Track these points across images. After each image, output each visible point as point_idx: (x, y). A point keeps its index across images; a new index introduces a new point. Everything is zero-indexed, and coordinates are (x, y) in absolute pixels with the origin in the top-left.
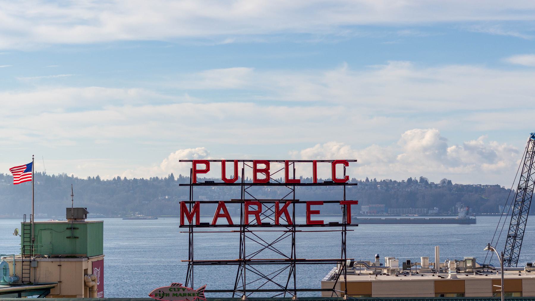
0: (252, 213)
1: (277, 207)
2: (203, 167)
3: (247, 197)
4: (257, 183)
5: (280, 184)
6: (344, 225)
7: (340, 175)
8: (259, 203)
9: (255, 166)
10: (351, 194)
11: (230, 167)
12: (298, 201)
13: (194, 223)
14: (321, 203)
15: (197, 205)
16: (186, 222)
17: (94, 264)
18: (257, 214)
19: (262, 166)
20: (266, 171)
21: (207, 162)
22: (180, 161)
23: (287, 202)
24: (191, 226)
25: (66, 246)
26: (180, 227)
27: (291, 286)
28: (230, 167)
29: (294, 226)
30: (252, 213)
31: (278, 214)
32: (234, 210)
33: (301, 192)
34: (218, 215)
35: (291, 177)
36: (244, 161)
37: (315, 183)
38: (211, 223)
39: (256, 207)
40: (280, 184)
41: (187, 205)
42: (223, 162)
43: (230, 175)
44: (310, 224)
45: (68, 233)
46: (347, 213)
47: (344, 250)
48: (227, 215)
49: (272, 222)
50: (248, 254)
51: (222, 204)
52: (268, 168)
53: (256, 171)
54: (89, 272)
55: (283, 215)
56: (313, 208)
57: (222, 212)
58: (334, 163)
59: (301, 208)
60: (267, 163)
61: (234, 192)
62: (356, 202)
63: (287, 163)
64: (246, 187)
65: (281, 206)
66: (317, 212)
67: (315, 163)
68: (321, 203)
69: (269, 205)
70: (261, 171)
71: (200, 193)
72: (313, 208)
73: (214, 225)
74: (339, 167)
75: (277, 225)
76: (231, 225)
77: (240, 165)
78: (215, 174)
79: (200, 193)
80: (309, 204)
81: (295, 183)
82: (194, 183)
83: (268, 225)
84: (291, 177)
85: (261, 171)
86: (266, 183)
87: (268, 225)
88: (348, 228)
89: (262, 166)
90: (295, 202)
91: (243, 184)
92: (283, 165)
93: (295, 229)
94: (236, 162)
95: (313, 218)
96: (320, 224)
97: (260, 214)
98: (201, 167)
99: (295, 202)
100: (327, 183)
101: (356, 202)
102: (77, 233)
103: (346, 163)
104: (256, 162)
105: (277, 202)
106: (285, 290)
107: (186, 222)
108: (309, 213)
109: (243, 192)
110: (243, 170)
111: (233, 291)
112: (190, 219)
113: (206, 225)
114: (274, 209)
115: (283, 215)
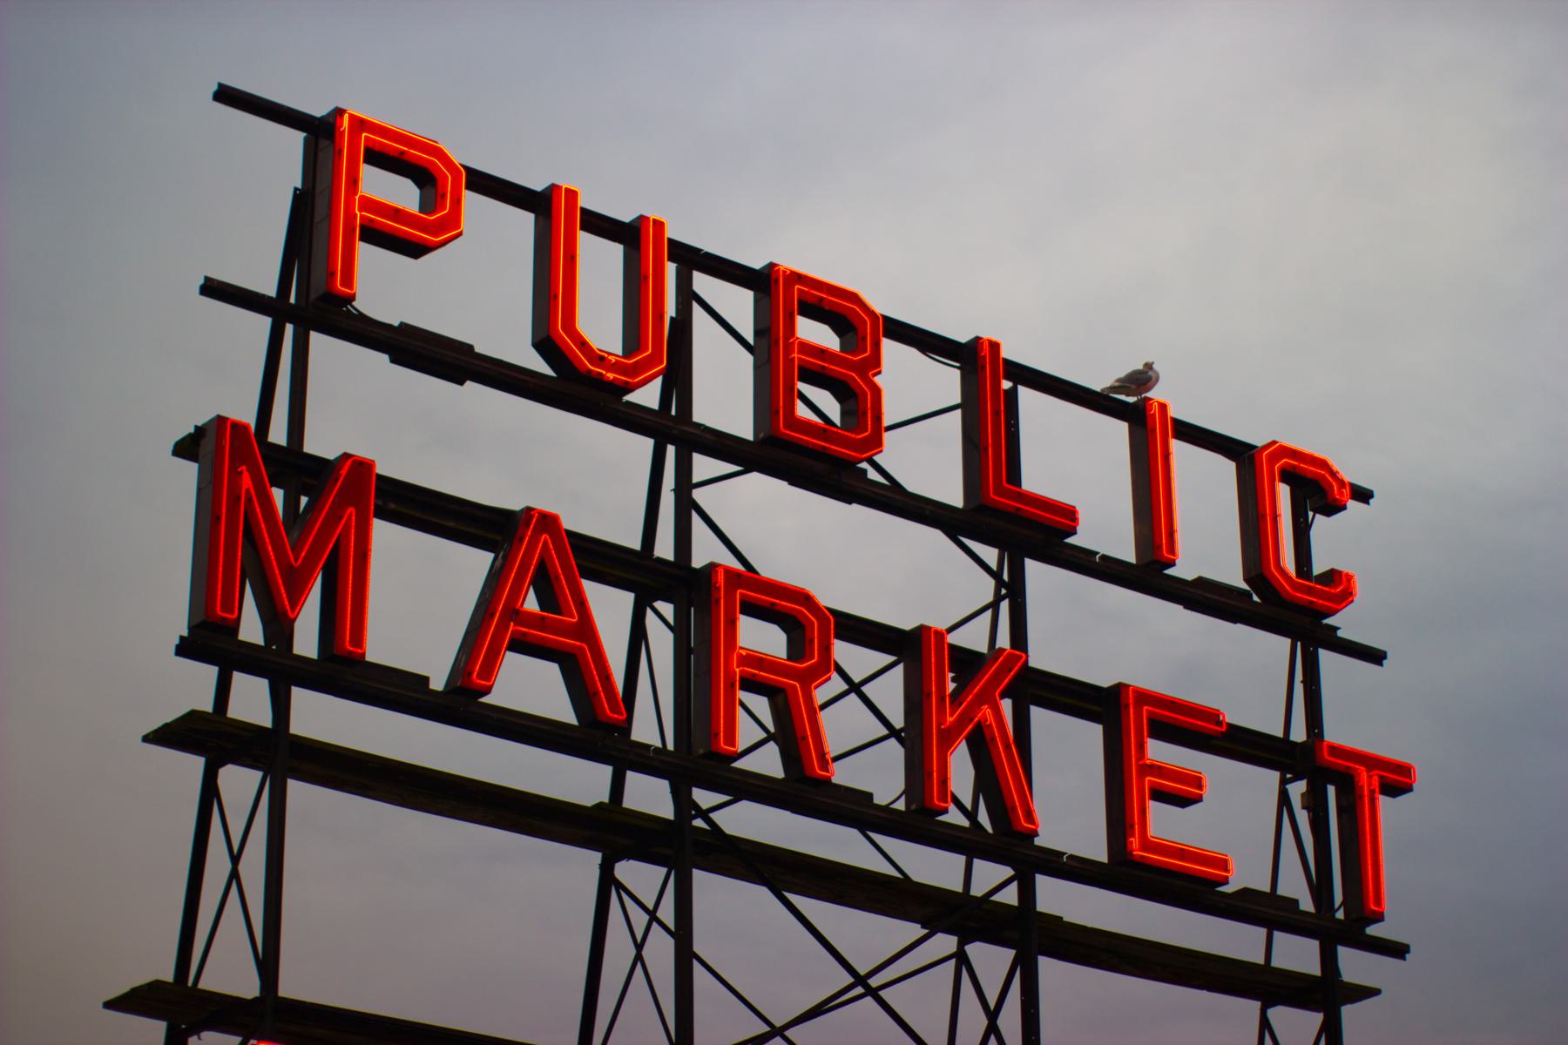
3: (706, 550)
4: (780, 452)
10: (1357, 713)
11: (599, 265)
13: (306, 641)
22: (226, 95)
26: (186, 649)
28: (599, 265)
30: (759, 676)
34: (492, 631)
36: (691, 259)
37: (1149, 573)
38: (438, 684)
64: (704, 466)
66: (1183, 792)
69: (854, 658)
71: (359, 409)
73: (462, 704)
76: (598, 732)
78: (476, 285)
83: (854, 810)
87: (854, 810)
88: (1354, 965)
93: (1028, 893)
95: (1164, 823)
96: (1191, 884)
97: (821, 694)
101: (1397, 779)
103: (1319, 490)
110: (682, 326)
113: (399, 691)
114: (890, 693)
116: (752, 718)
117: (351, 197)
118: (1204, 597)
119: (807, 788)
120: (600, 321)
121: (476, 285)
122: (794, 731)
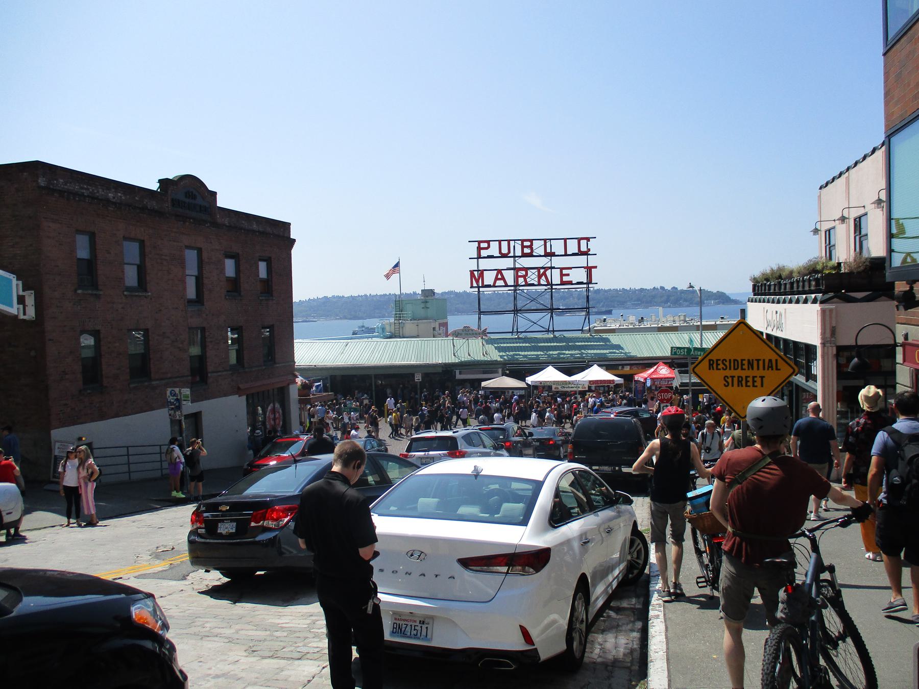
0: (521, 276)
1: (539, 272)
2: (485, 245)
3: (518, 266)
4: (524, 255)
5: (540, 256)
6: (587, 283)
7: (584, 249)
8: (526, 269)
9: (522, 244)
11: (504, 245)
12: (554, 268)
14: (570, 268)
15: (481, 273)
16: (475, 284)
17: (440, 325)
18: (525, 277)
19: (528, 244)
20: (531, 247)
21: (488, 242)
23: (546, 269)
24: (479, 287)
25: (421, 312)
27: (551, 329)
28: (504, 245)
29: (552, 285)
30: (521, 276)
31: (540, 277)
32: (509, 276)
33: (557, 262)
34: (497, 279)
35: (548, 251)
37: (566, 255)
39: (524, 273)
40: (540, 256)
41: (476, 273)
42: (500, 241)
43: (505, 251)
44: (563, 283)
45: (423, 305)
46: (589, 276)
47: (588, 301)
48: (503, 278)
49: (536, 283)
50: (520, 305)
51: (499, 271)
52: (532, 244)
53: (523, 247)
54: (437, 329)
55: (543, 278)
56: (565, 272)
57: (499, 276)
58: (579, 240)
59: (556, 273)
60: (531, 241)
61: (508, 263)
62: (595, 267)
63: (545, 240)
65: (542, 271)
66: (568, 275)
67: (565, 240)
68: (570, 268)
69: (533, 271)
70: (527, 247)
71: (484, 264)
72: (565, 272)
73: (494, 286)
74: (583, 242)
75: (539, 284)
76: (506, 285)
77: (512, 243)
79: (484, 264)
80: (562, 269)
81: (552, 254)
82: (479, 257)
84: (548, 251)
85: (527, 247)
86: (530, 255)
89: (528, 244)
90: (552, 268)
91: (514, 257)
92: (543, 242)
94: (509, 241)
95: (565, 279)
96: (570, 283)
98: (483, 245)
99: (552, 268)
100: (574, 254)
101: (595, 267)
102: (428, 305)
103: (588, 239)
104: (523, 241)
105: (538, 269)
106: (548, 331)
107: (475, 284)
108: (562, 275)
109: (515, 261)
111: (512, 332)
112: (477, 282)
115: (543, 278)
116: (521, 280)
117: (481, 246)
118: (574, 254)
119: (527, 285)
120: (505, 251)
121: (494, 250)
122: (525, 280)
